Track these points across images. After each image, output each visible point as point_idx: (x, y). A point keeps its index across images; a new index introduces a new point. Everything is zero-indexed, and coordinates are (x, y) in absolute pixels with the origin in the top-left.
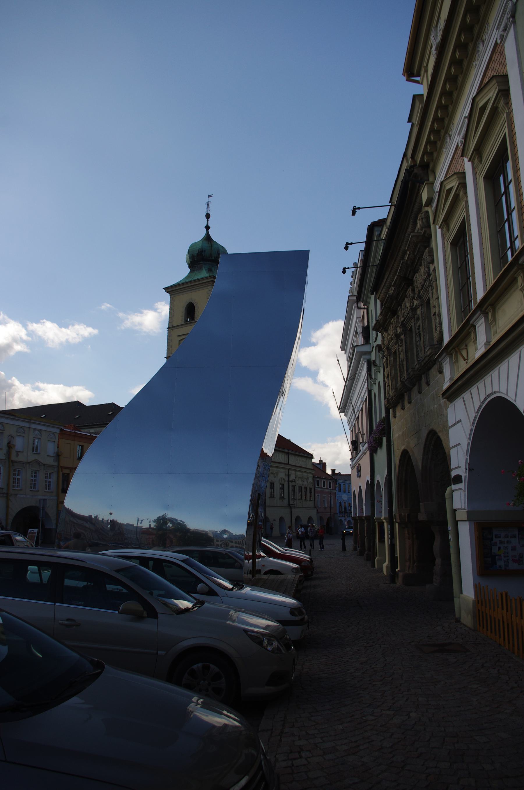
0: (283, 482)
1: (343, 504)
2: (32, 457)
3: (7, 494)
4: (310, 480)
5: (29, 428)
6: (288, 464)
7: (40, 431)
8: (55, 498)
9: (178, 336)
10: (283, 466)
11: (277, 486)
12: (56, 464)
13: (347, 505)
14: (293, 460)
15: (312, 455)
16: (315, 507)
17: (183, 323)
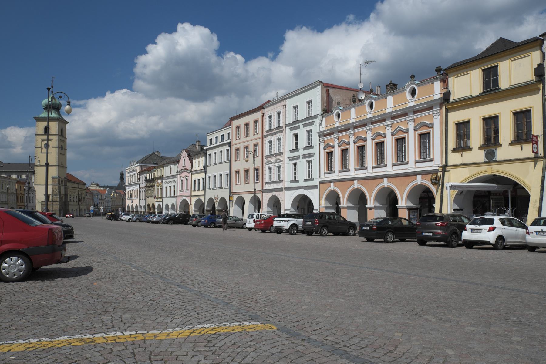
0: (77, 195)
1: (95, 203)
2: (12, 191)
3: (8, 203)
4: (85, 194)
5: (11, 182)
6: (78, 188)
7: (13, 182)
8: (16, 204)
9: (41, 139)
10: (84, 190)
11: (72, 197)
12: (16, 193)
13: (97, 204)
14: (81, 186)
15: (85, 184)
16: (86, 205)
17: (44, 134)
